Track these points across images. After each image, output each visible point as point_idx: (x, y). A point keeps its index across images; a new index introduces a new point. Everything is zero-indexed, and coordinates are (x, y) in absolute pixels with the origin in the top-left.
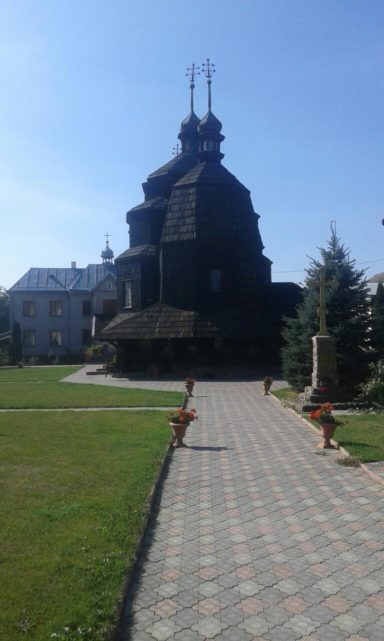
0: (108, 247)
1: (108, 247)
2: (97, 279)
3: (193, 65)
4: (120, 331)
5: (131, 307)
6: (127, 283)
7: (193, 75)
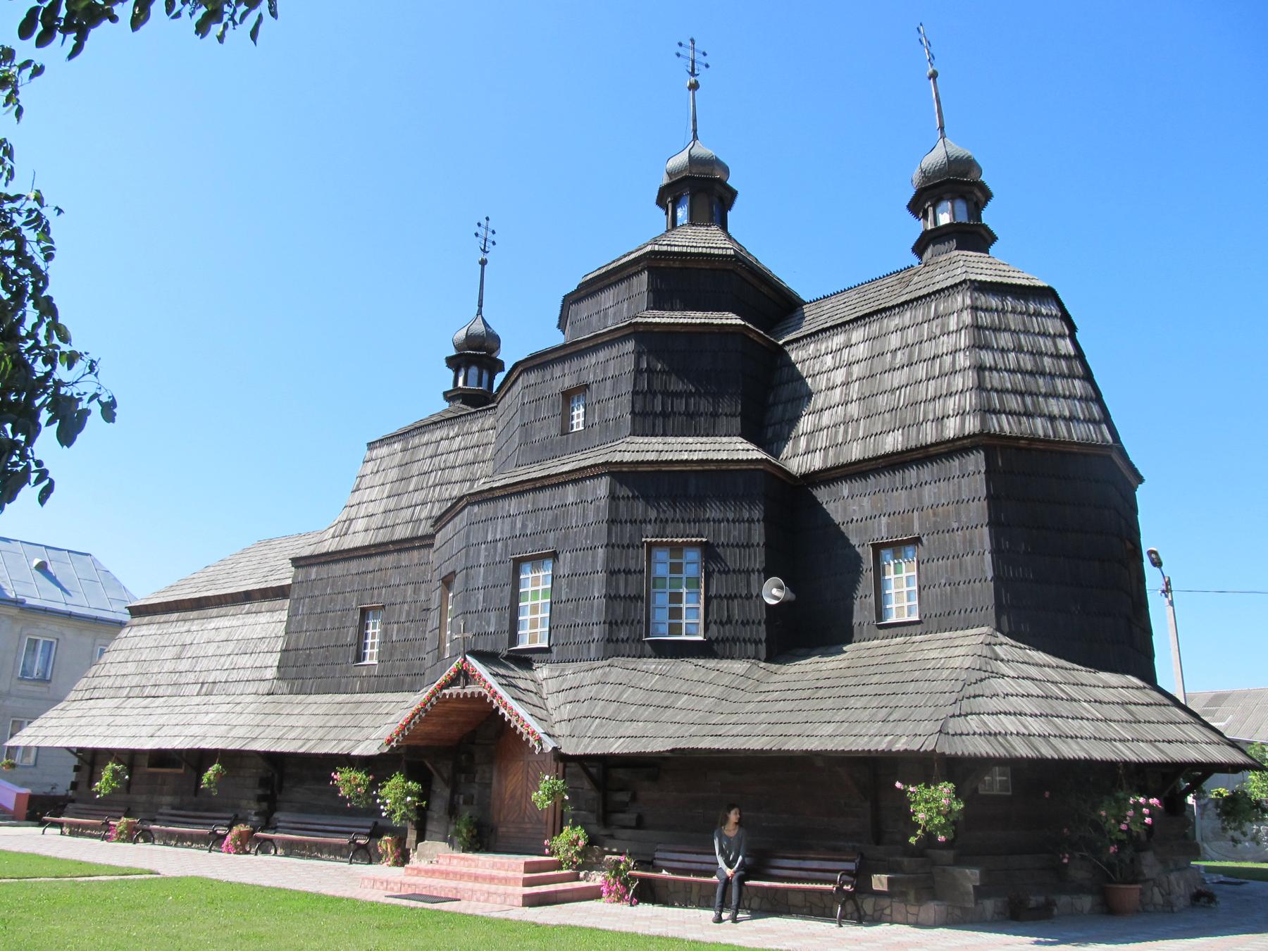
3: (693, 41)
7: (693, 62)
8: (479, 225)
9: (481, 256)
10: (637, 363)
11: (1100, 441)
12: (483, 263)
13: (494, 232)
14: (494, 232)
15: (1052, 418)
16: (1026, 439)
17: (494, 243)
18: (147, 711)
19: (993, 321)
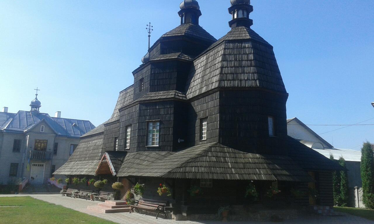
0: (36, 99)
1: (36, 99)
2: (27, 123)
4: (193, 169)
5: (158, 146)
6: (151, 124)
8: (147, 25)
9: (148, 34)
10: (151, 72)
11: (255, 86)
12: (149, 36)
13: (152, 27)
14: (152, 27)
15: (241, 80)
16: (231, 87)
17: (152, 30)
18: (78, 165)
19: (230, 52)
